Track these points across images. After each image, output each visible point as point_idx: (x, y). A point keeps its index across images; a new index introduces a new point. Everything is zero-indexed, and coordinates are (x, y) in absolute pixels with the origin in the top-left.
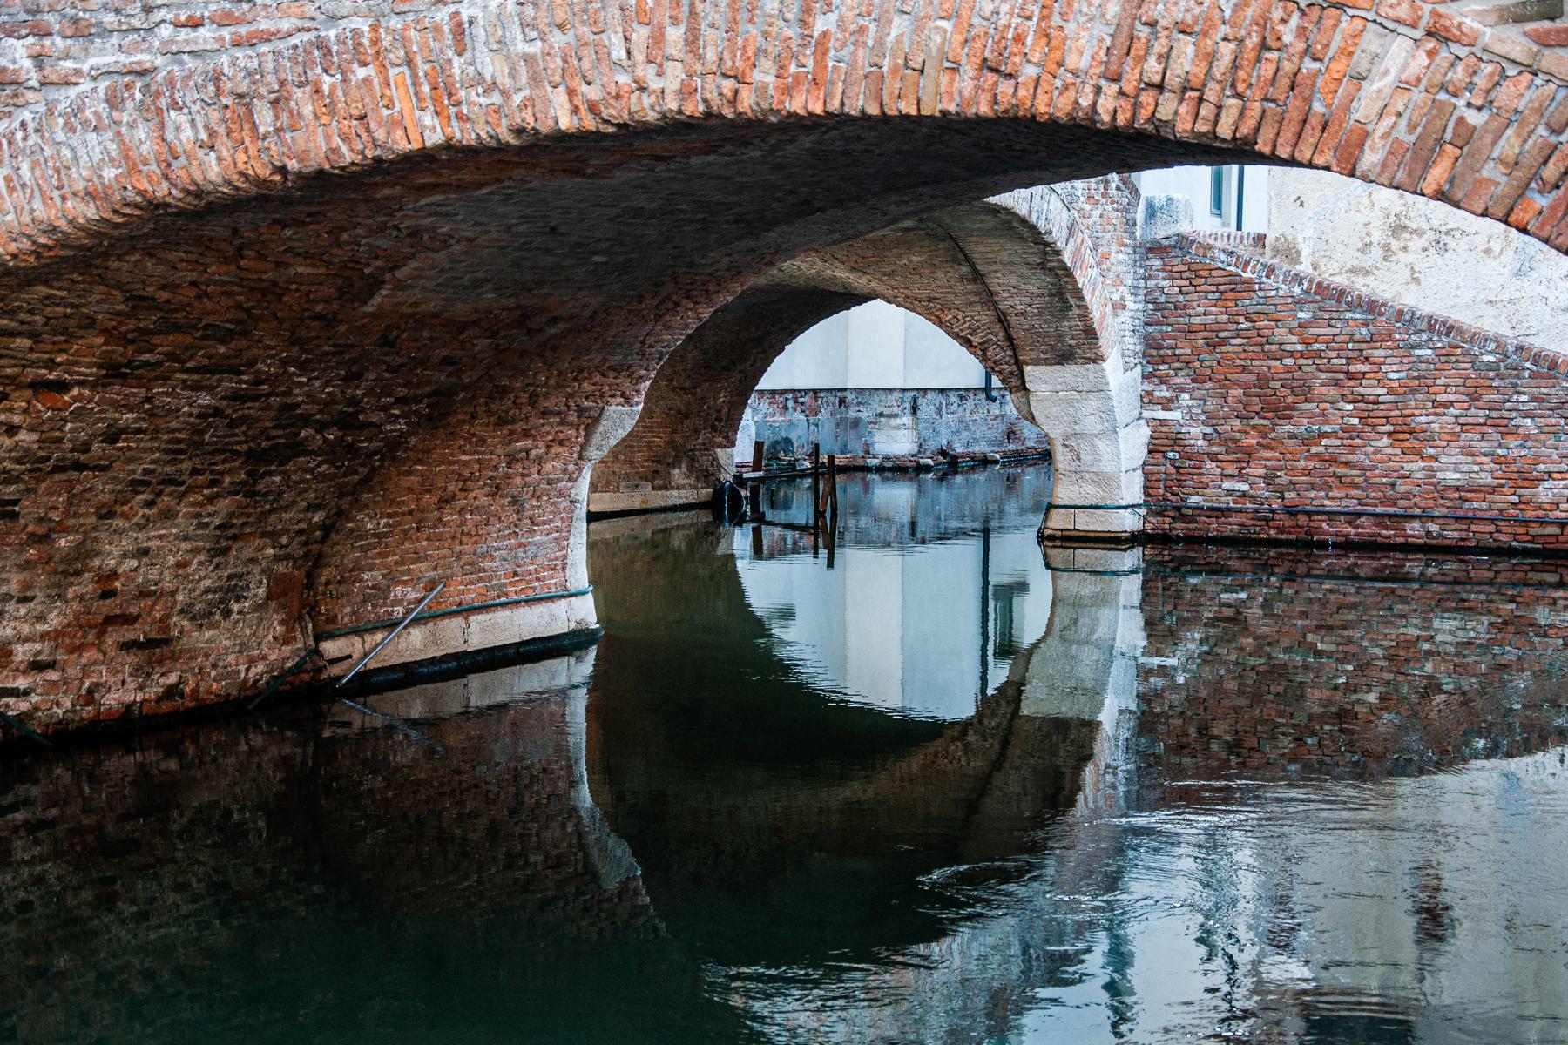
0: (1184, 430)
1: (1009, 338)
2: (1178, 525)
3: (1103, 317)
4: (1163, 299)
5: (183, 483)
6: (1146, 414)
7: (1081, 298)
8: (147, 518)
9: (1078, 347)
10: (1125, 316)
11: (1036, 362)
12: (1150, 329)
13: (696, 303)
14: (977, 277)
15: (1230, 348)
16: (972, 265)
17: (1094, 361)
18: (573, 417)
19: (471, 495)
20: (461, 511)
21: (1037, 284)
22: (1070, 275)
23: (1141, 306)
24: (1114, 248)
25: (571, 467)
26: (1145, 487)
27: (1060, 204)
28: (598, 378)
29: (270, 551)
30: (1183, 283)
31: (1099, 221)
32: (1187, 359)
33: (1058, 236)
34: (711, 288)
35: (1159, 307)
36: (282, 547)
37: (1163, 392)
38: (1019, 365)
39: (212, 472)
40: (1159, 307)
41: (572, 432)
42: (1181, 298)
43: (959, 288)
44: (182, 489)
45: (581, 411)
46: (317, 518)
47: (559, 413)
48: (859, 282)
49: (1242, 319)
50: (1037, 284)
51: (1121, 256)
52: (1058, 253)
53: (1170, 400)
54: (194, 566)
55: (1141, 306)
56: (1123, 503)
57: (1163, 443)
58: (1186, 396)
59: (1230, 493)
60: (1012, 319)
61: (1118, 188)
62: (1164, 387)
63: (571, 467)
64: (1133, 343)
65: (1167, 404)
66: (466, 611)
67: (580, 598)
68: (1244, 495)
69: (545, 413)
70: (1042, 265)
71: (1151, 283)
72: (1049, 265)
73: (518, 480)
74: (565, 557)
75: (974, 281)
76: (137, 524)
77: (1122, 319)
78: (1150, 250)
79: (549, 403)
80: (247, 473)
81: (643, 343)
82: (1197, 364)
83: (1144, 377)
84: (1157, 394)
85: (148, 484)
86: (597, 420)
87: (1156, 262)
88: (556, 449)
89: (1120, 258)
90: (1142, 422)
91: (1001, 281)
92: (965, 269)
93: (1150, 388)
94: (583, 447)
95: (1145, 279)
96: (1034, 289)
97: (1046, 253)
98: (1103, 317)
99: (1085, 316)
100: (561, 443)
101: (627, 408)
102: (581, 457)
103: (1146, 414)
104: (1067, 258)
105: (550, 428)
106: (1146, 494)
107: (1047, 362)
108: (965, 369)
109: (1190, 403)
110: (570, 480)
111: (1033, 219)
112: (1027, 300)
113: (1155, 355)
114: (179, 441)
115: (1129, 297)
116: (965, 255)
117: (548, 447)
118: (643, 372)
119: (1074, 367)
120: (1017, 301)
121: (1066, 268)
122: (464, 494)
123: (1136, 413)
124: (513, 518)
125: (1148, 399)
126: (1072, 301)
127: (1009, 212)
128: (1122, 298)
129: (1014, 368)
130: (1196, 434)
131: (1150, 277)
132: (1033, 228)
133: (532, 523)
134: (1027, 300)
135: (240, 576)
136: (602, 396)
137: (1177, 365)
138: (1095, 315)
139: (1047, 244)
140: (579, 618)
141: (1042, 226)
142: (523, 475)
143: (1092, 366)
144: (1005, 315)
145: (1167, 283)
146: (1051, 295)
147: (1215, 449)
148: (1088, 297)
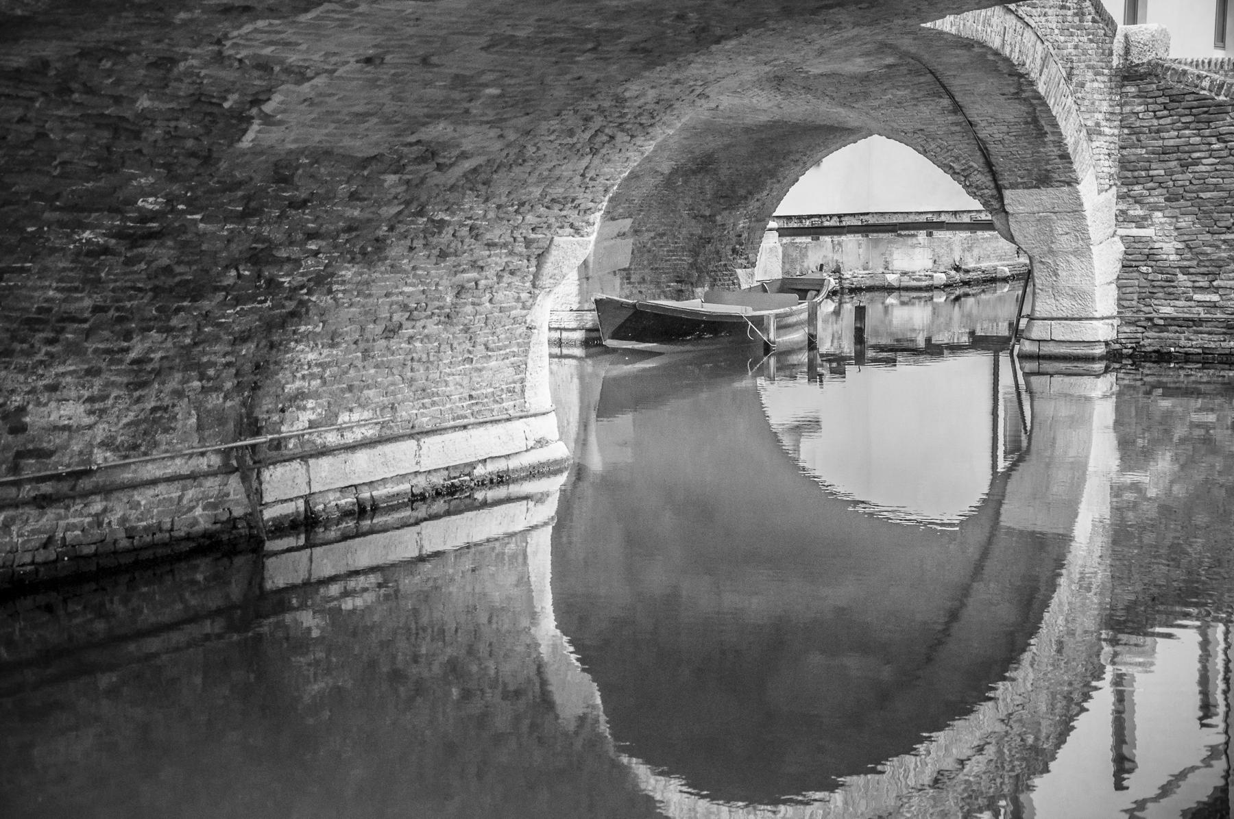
0: (1157, 245)
1: (989, 165)
2: (1150, 334)
3: (1076, 143)
4: (1138, 124)
5: (85, 321)
6: (1121, 232)
7: (1056, 125)
8: (51, 355)
9: (1052, 170)
10: (1100, 142)
11: (1014, 186)
12: (1125, 152)
13: (632, 136)
14: (957, 108)
15: (1203, 168)
16: (952, 97)
17: (1069, 184)
18: (520, 248)
19: (419, 324)
20: (411, 339)
21: (1013, 112)
22: (1045, 104)
23: (1116, 131)
24: (1090, 75)
25: (524, 296)
26: (1119, 299)
27: (1034, 38)
28: (542, 210)
29: (196, 384)
30: (1158, 107)
31: (1074, 52)
32: (1160, 179)
33: (1032, 67)
34: (644, 120)
35: (1134, 131)
36: (209, 379)
37: (1138, 211)
38: (999, 188)
39: (118, 309)
40: (1134, 131)
41: (516, 262)
42: (1155, 122)
43: (940, 120)
44: (86, 326)
45: (528, 243)
46: (247, 349)
47: (505, 245)
48: (849, 117)
49: (1214, 140)
50: (1013, 112)
51: (1096, 85)
52: (1032, 83)
53: (1144, 218)
54: (110, 402)
55: (1116, 131)
56: (1097, 315)
57: (1137, 259)
58: (1159, 214)
59: (1200, 303)
60: (992, 147)
61: (1094, 21)
62: (1138, 206)
63: (524, 296)
64: (1108, 166)
65: (1140, 222)
66: (417, 434)
67: (540, 418)
68: (1214, 306)
69: (490, 245)
70: (1017, 96)
71: (1127, 109)
72: (1024, 95)
73: (469, 309)
74: (522, 381)
75: (955, 112)
76: (41, 362)
77: (1097, 144)
78: (1125, 78)
79: (493, 235)
80: (157, 310)
81: (583, 175)
82: (1171, 183)
83: (1119, 197)
84: (1131, 212)
85: (46, 322)
86: (547, 250)
87: (1132, 89)
88: (507, 278)
89: (1097, 87)
90: (1117, 239)
91: (978, 111)
92: (946, 102)
93: (1124, 207)
94: (536, 276)
95: (1122, 105)
96: (1010, 118)
97: (1020, 84)
98: (1076, 143)
99: (1060, 142)
100: (512, 273)
101: (578, 238)
102: (534, 286)
103: (1121, 232)
104: (1041, 89)
105: (498, 259)
106: (1119, 306)
107: (1027, 186)
108: (942, 192)
109: (1163, 220)
110: (524, 308)
111: (1007, 51)
112: (1005, 129)
113: (1129, 174)
114: (72, 280)
115: (1104, 123)
116: (944, 87)
117: (499, 277)
118: (591, 205)
119: (1050, 190)
120: (994, 129)
121: (1040, 98)
122: (407, 324)
123: (1111, 231)
124: (468, 346)
125: (1123, 218)
126: (1047, 128)
127: (982, 45)
128: (1098, 124)
129: (995, 192)
130: (1169, 249)
131: (1126, 103)
132: (1007, 60)
133: (487, 349)
134: (1005, 129)
135: (166, 409)
136: (549, 227)
137: (1151, 185)
138: (1069, 141)
139: (1021, 76)
140: (538, 437)
141: (1015, 57)
142: (473, 304)
143: (1066, 189)
144: (984, 143)
145: (1141, 108)
146: (1026, 123)
147: (1186, 263)
148: (1062, 124)
